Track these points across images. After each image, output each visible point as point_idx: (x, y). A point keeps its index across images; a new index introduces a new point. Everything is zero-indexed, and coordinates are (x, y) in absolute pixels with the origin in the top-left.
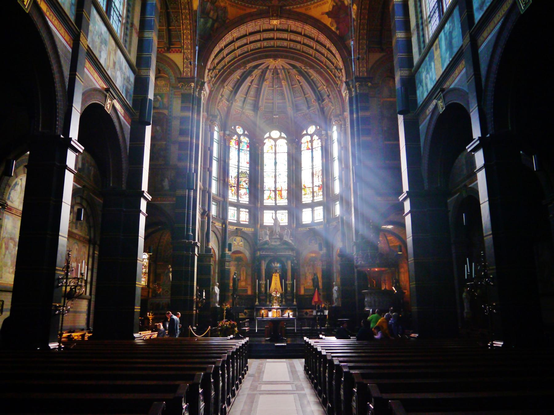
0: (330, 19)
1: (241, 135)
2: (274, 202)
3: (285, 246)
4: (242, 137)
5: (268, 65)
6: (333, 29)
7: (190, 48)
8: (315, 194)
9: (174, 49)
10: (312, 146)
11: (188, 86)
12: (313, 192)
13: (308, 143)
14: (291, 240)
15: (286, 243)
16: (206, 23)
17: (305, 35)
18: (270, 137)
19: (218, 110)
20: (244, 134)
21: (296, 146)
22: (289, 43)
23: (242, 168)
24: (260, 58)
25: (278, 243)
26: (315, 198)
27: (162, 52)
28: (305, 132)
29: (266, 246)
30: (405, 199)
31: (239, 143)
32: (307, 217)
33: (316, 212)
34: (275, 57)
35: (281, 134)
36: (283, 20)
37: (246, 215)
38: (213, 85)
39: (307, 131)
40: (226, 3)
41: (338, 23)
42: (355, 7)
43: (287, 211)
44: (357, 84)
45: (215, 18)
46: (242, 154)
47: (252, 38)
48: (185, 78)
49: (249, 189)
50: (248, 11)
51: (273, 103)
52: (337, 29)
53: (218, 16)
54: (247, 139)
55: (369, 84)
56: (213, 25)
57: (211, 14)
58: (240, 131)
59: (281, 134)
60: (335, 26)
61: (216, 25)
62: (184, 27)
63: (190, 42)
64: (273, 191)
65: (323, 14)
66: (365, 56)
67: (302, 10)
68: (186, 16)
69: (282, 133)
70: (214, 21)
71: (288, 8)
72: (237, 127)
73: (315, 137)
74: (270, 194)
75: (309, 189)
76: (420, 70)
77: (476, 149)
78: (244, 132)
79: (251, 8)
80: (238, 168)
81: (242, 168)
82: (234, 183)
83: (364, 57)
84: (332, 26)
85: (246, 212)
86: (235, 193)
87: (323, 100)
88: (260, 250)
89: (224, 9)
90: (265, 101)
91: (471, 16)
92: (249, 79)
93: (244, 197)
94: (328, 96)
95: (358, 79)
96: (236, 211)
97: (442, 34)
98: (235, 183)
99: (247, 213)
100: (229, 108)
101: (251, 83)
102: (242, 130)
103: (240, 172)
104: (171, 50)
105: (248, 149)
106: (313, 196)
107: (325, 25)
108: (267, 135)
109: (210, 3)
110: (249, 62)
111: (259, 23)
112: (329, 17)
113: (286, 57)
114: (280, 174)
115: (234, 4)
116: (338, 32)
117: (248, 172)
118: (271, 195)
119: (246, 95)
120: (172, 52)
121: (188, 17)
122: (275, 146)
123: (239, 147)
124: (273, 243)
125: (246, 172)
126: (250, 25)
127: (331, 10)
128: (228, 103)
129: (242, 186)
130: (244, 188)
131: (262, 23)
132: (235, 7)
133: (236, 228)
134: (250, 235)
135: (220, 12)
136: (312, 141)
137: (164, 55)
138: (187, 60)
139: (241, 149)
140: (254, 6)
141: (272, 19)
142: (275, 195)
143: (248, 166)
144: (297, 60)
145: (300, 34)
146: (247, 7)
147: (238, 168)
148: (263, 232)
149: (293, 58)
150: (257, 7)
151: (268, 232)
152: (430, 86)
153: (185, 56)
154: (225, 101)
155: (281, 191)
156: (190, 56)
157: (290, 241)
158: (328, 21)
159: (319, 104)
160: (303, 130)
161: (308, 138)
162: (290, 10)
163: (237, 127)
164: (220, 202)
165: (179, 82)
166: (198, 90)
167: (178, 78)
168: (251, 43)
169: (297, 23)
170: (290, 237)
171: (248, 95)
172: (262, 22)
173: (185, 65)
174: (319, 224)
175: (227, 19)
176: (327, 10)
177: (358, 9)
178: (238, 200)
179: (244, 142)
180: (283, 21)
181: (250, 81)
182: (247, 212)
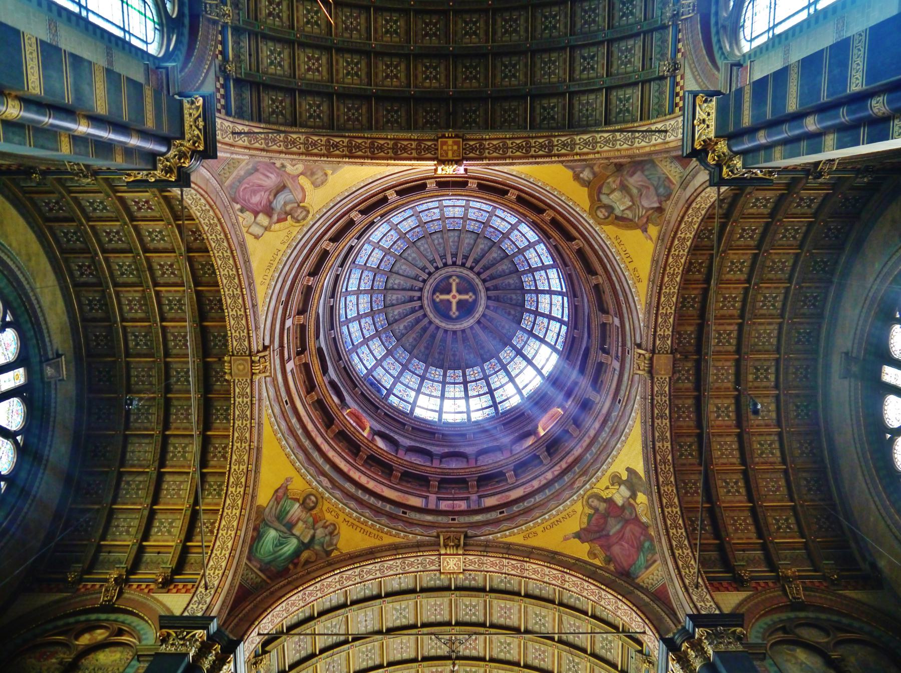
0: (586, 547)
6: (597, 562)
7: (223, 567)
9: (181, 586)
11: (183, 639)
16: (280, 544)
27: (146, 591)
36: (471, 557)
40: (337, 516)
41: (607, 548)
42: (641, 498)
44: (698, 632)
45: (306, 540)
50: (388, 540)
52: (609, 560)
53: (313, 537)
55: (739, 630)
56: (297, 553)
57: (300, 524)
60: (602, 555)
61: (305, 555)
62: (223, 523)
63: (227, 556)
65: (566, 539)
66: (700, 580)
67: (516, 538)
68: (234, 500)
70: (304, 546)
71: (482, 538)
83: (698, 583)
84: (595, 556)
89: (333, 531)
95: (698, 619)
104: (172, 587)
107: (578, 560)
109: (301, 505)
111: (411, 564)
112: (583, 542)
115: (355, 522)
120: (175, 590)
121: (240, 502)
126: (390, 568)
127: (583, 526)
131: (420, 569)
132: (359, 529)
137: (152, 597)
138: (206, 589)
140: (402, 534)
141: (446, 554)
150: (411, 536)
153: (203, 582)
156: (216, 583)
158: (580, 550)
162: (487, 541)
165: (161, 628)
166: (214, 662)
167: (161, 618)
169: (505, 561)
172: (422, 563)
173: (195, 599)
175: (337, 549)
176: (577, 529)
177: (649, 494)
180: (472, 562)
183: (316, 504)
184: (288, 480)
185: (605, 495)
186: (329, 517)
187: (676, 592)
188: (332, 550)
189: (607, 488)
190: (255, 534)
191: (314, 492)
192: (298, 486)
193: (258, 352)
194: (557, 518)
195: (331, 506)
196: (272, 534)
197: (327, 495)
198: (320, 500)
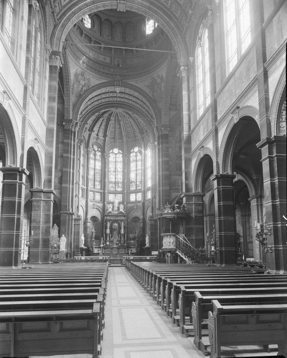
3: (121, 214)
4: (97, 152)
5: (112, 111)
8: (137, 186)
10: (136, 159)
12: (136, 185)
14: (124, 211)
15: (121, 213)
17: (134, 97)
18: (113, 152)
19: (84, 136)
20: (98, 150)
21: (128, 158)
22: (125, 100)
24: (108, 107)
25: (116, 213)
26: (137, 188)
28: (132, 151)
29: (110, 214)
30: (183, 197)
31: (95, 155)
32: (133, 198)
33: (137, 196)
34: (117, 107)
35: (119, 151)
38: (81, 122)
39: (134, 150)
43: (122, 195)
45: (83, 85)
46: (97, 162)
47: (103, 96)
48: (66, 120)
49: (101, 182)
51: (115, 133)
58: (96, 148)
59: (119, 151)
67: (134, 83)
69: (120, 151)
71: (125, 81)
73: (138, 154)
76: (194, 132)
77: (214, 180)
78: (98, 149)
79: (104, 79)
87: (143, 134)
88: (107, 216)
90: (110, 132)
91: (216, 117)
92: (101, 119)
93: (98, 186)
94: (146, 131)
97: (204, 118)
99: (99, 195)
100: (90, 135)
101: (103, 121)
103: (96, 172)
106: (136, 187)
108: (111, 151)
110: (102, 109)
113: (123, 108)
114: (118, 174)
116: (153, 98)
119: (100, 127)
122: (116, 157)
124: (114, 213)
128: (89, 132)
133: (93, 204)
134: (101, 207)
135: (86, 81)
136: (136, 156)
142: (115, 185)
144: (130, 110)
145: (131, 95)
146: (102, 79)
148: (109, 206)
149: (126, 108)
151: (111, 207)
152: (198, 143)
154: (87, 131)
155: (118, 183)
157: (124, 212)
159: (141, 135)
160: (131, 150)
161: (135, 154)
163: (94, 146)
164: (84, 189)
168: (103, 98)
170: (123, 209)
171: (101, 128)
174: (139, 202)
181: (102, 119)
183: (84, 74)
184: (77, 70)
185: (155, 78)
186: (88, 77)
187: (163, 113)
188: (90, 86)
189: (156, 77)
190: (72, 88)
191: (83, 71)
192: (79, 71)
193: (65, 45)
194: (143, 80)
195: (88, 73)
196: (76, 85)
197: (87, 70)
198: (85, 72)
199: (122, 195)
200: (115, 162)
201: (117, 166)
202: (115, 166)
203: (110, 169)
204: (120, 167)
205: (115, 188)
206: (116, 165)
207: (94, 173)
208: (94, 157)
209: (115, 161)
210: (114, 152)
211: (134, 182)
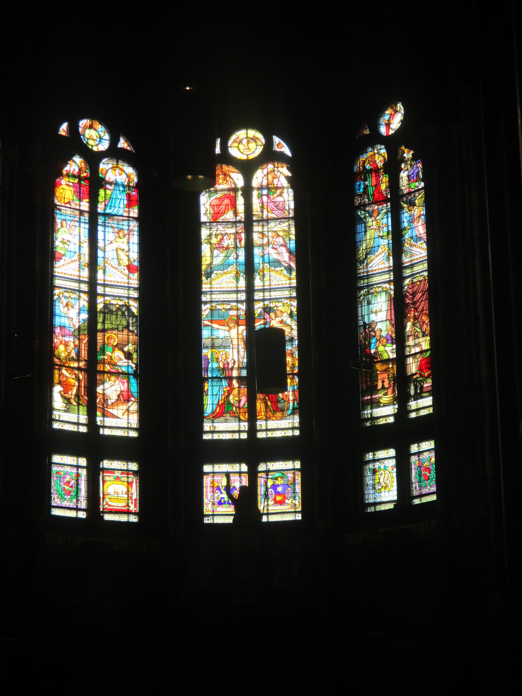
1: (102, 155)
2: (245, 426)
13: (378, 177)
23: (108, 290)
37: (130, 484)
39: (375, 128)
54: (130, 170)
64: (239, 379)
69: (276, 140)
72: (83, 123)
74: (230, 392)
75: (385, 367)
80: (92, 295)
81: (108, 290)
82: (73, 354)
85: (127, 472)
86: (78, 395)
93: (119, 411)
96: (83, 472)
98: (78, 354)
99: (132, 478)
102: (107, 137)
105: (134, 212)
117: (134, 307)
118: (232, 399)
123: (94, 202)
125: (128, 308)
129: (108, 368)
130: (118, 374)
139: (105, 215)
143: (134, 280)
147: (92, 295)
178: (92, 424)
179: (116, 184)
182: (135, 473)
199: (298, 465)
200: (241, 227)
201: (257, 251)
202: (242, 253)
203: (209, 275)
204: (285, 257)
205: (252, 420)
206: (249, 247)
207: (85, 316)
208: (85, 205)
209: (241, 216)
210: (234, 152)
211: (388, 361)
